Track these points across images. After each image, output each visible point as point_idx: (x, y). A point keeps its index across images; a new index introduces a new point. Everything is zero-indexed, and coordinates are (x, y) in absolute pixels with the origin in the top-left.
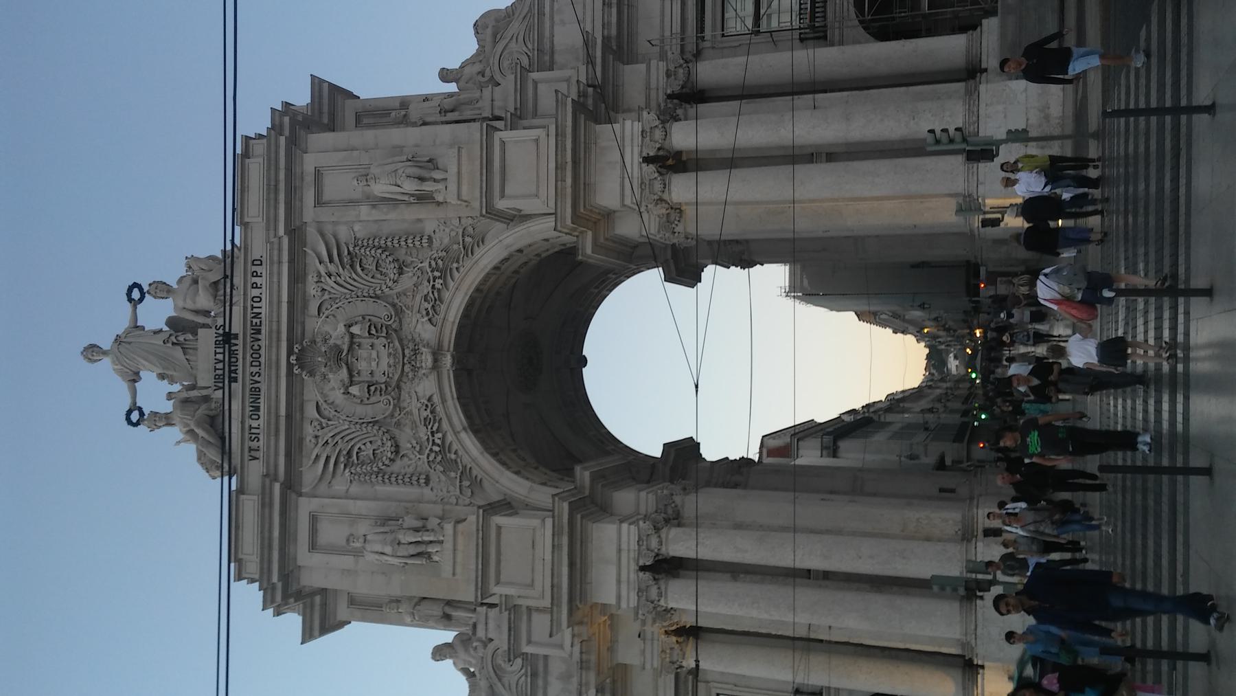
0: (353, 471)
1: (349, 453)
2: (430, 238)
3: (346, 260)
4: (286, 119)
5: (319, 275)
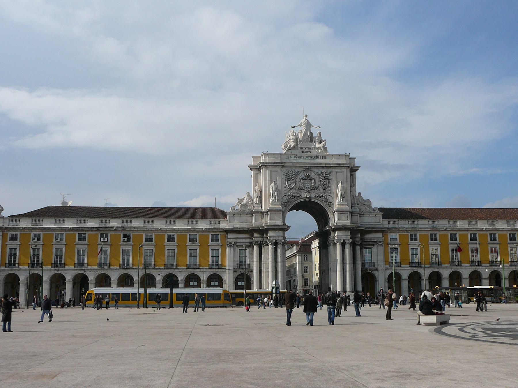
0: (286, 180)
1: (289, 179)
2: (330, 196)
3: (326, 178)
4: (352, 166)
5: (323, 172)
